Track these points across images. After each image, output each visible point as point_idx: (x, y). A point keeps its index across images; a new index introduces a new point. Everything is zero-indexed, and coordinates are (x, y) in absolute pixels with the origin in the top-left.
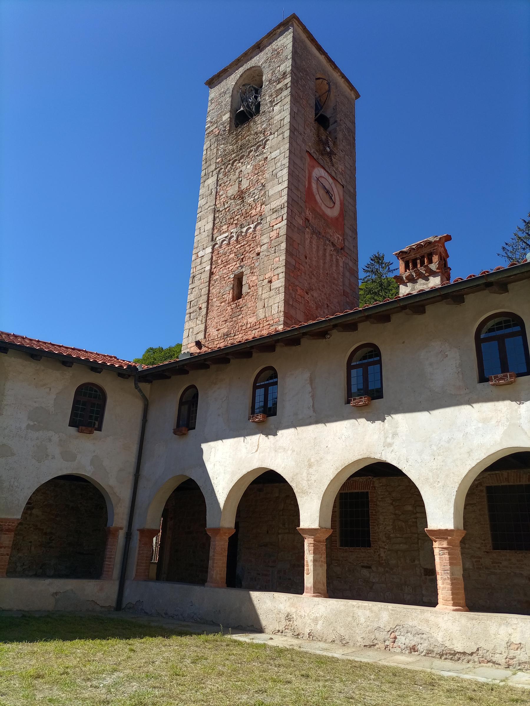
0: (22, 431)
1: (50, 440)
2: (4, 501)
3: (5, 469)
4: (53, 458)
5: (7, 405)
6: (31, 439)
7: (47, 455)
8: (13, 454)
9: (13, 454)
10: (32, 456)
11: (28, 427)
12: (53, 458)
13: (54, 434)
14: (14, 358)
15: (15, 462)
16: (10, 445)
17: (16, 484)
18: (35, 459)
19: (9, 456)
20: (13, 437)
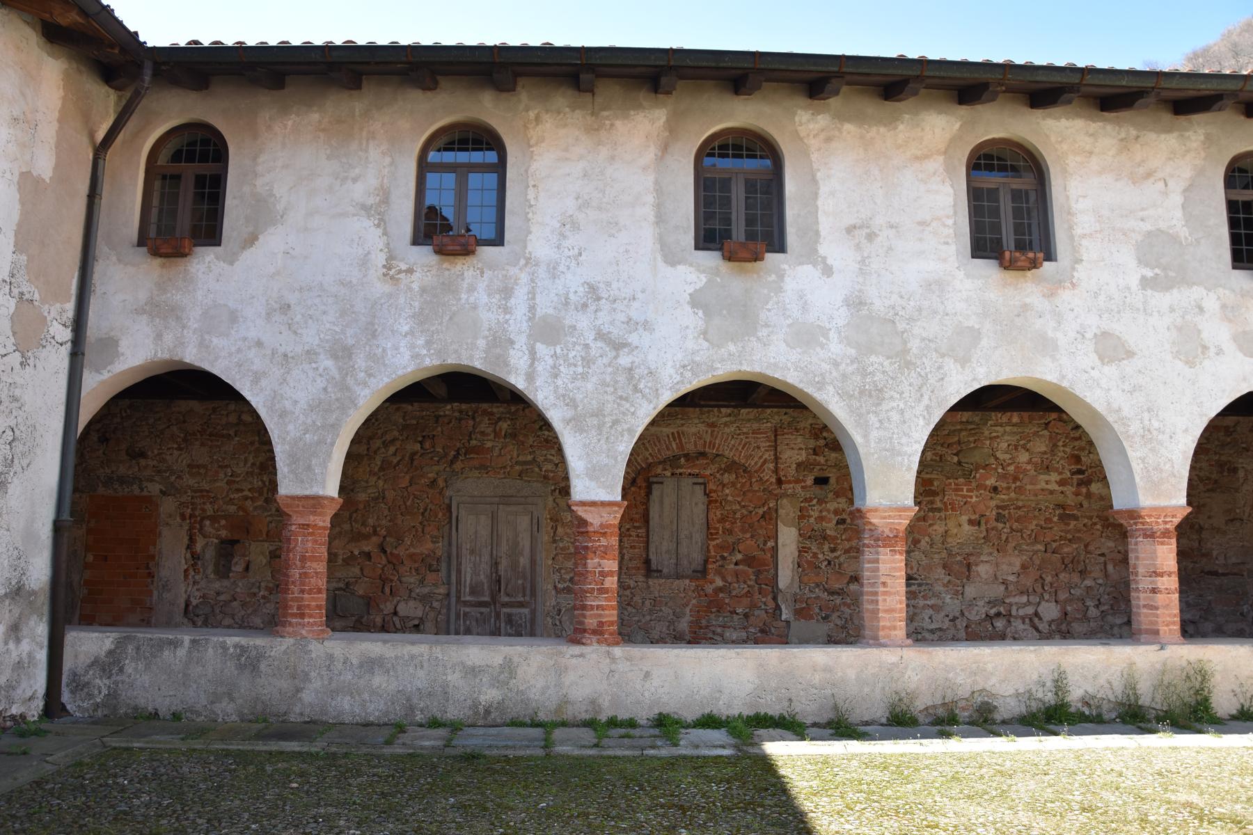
0: (1134, 296)
1: (1201, 309)
2: (1142, 466)
3: (1123, 391)
4: (1220, 352)
5: (1084, 236)
6: (1159, 312)
7: (1205, 348)
8: (1130, 354)
9: (1130, 354)
10: (1172, 353)
11: (1145, 283)
12: (1220, 352)
13: (1204, 292)
14: (1067, 119)
15: (1140, 371)
16: (1117, 333)
17: (1156, 424)
18: (1180, 360)
19: (1123, 359)
20: (1119, 312)
